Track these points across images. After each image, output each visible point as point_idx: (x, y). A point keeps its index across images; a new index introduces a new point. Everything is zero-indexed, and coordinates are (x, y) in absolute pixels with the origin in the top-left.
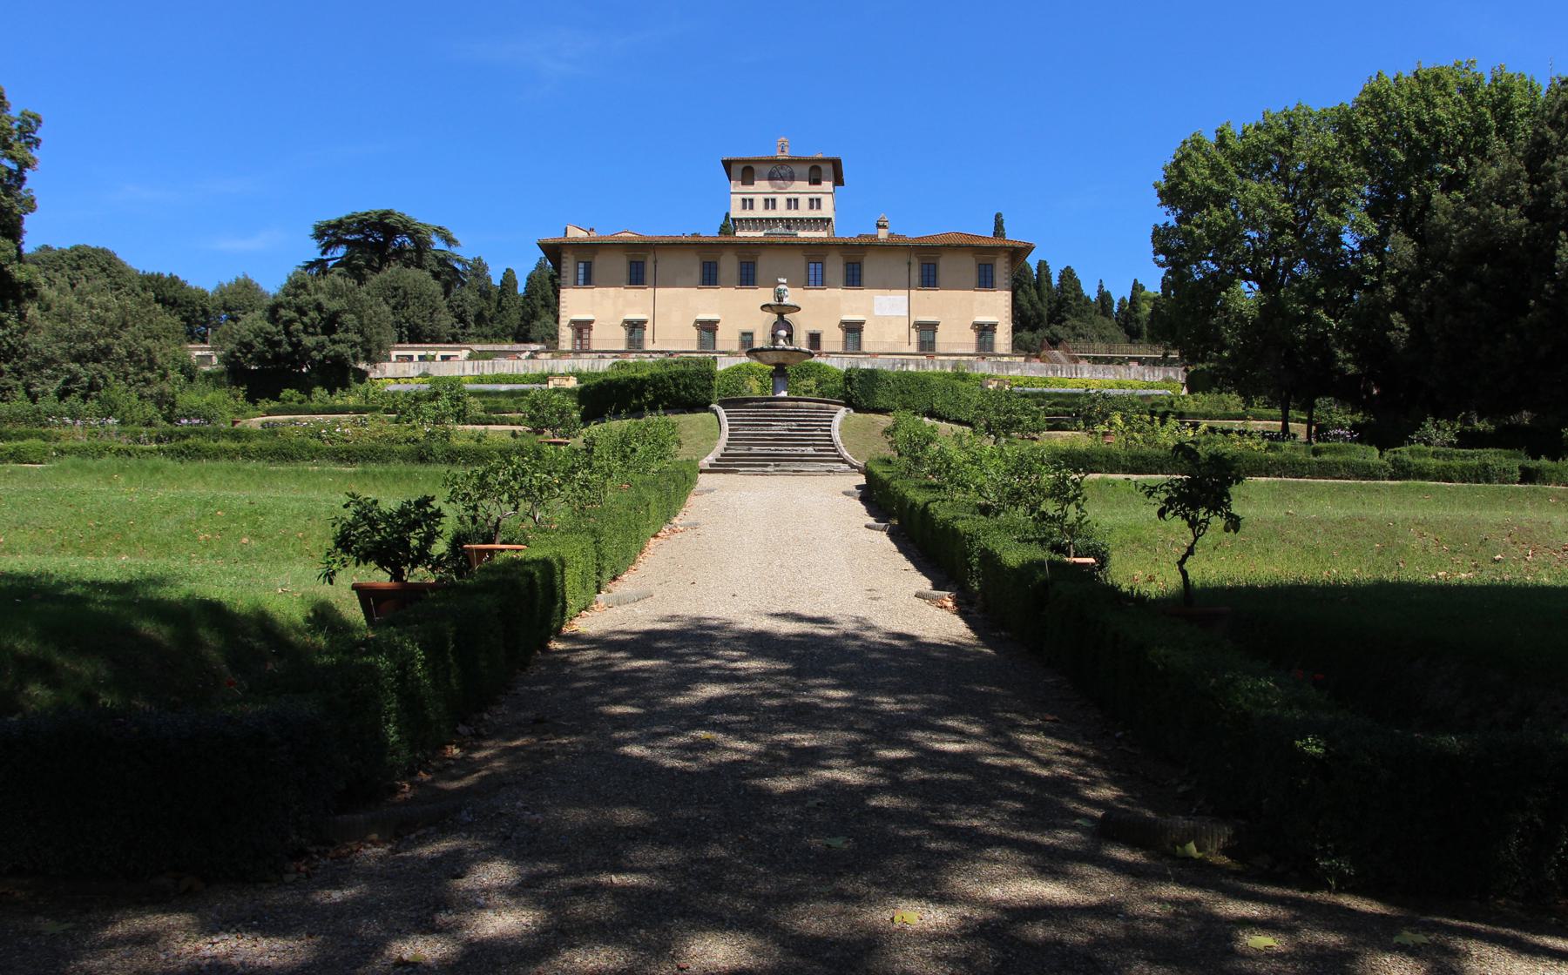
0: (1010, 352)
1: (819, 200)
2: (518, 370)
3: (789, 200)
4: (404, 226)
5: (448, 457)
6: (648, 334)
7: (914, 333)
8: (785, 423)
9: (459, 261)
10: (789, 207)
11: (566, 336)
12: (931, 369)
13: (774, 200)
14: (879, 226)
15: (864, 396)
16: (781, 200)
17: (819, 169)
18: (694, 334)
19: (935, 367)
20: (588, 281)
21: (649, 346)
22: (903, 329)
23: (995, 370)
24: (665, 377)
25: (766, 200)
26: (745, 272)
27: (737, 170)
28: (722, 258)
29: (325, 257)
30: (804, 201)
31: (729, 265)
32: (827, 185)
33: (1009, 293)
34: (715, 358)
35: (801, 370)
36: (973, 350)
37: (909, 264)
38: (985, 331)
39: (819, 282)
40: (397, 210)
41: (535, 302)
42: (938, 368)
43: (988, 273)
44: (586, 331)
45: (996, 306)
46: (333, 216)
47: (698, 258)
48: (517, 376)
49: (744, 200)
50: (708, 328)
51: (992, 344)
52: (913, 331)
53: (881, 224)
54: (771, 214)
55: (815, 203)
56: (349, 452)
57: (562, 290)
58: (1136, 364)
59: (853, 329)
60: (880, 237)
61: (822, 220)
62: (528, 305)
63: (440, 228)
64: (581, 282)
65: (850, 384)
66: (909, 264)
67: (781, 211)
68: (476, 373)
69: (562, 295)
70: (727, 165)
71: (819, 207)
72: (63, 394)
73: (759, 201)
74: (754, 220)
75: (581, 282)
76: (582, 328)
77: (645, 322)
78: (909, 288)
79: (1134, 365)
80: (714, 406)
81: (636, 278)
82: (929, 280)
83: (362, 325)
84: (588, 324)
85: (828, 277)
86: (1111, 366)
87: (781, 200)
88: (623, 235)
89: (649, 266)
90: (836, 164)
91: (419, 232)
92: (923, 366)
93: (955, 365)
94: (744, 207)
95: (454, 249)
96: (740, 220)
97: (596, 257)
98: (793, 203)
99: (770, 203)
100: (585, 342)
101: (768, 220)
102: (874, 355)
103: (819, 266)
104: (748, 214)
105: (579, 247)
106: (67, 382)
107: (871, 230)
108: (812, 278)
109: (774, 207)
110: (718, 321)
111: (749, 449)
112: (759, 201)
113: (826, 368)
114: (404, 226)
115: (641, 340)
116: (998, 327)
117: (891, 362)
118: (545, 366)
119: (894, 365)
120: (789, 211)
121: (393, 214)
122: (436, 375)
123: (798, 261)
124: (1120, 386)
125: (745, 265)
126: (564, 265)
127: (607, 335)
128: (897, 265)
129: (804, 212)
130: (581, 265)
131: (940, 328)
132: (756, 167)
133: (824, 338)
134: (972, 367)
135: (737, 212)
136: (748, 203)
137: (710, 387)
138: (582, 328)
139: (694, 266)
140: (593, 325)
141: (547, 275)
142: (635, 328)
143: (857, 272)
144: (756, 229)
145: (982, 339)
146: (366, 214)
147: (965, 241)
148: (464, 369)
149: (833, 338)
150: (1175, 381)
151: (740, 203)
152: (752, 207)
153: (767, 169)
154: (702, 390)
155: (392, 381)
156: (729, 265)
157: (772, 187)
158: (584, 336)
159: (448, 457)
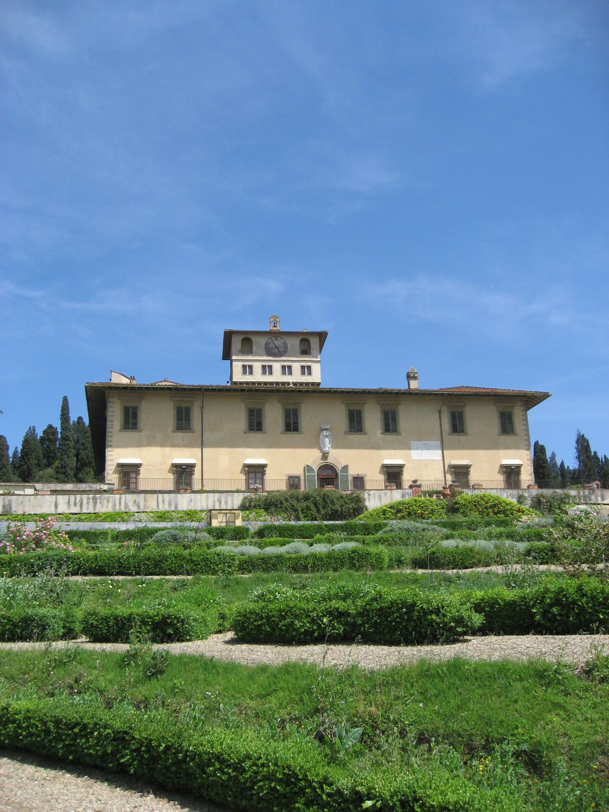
2: (126, 506)
11: (112, 476)
13: (270, 367)
16: (277, 367)
17: (308, 341)
25: (264, 367)
30: (296, 367)
37: (440, 412)
38: (511, 474)
44: (133, 475)
61: (313, 384)
66: (440, 412)
71: (310, 373)
73: (257, 367)
76: (129, 472)
77: (192, 466)
81: (183, 421)
87: (277, 367)
98: (287, 370)
109: (271, 373)
110: (264, 466)
112: (257, 367)
116: (523, 469)
131: (472, 470)
132: (254, 339)
138: (129, 472)
140: (141, 469)
148: (56, 506)
149: (375, 479)
151: (240, 369)
152: (251, 373)
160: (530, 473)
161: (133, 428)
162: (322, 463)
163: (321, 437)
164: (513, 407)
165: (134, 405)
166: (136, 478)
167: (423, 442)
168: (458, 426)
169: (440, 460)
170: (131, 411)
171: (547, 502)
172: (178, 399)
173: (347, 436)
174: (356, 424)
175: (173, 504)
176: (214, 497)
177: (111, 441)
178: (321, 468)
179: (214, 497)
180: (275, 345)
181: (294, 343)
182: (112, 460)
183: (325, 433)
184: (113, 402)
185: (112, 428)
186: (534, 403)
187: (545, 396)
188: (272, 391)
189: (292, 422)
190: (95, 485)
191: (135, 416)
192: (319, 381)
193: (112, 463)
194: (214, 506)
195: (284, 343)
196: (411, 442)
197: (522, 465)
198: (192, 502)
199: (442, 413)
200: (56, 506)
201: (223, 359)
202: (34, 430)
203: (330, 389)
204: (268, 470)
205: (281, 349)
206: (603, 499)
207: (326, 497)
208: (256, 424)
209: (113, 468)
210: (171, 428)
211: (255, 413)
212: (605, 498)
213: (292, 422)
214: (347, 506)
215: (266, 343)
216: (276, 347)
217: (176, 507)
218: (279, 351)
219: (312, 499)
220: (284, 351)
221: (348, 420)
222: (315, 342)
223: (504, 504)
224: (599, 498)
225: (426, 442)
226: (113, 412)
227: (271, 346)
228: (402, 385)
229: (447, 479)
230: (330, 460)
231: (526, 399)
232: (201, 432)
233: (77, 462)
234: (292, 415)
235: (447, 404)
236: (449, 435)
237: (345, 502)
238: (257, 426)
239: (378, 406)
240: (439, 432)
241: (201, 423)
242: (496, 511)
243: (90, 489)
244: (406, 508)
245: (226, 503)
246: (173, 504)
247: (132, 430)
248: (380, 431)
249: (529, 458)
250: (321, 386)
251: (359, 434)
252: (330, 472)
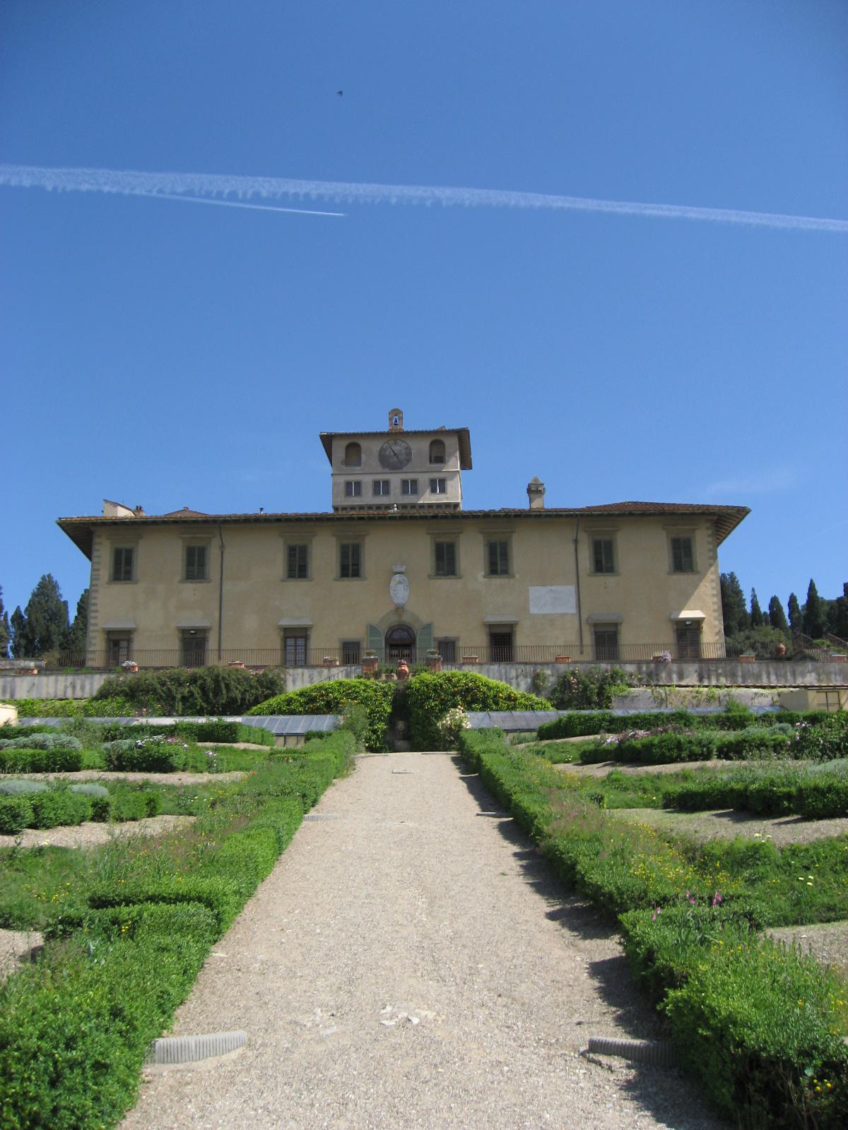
3: (405, 483)
7: (588, 639)
11: (96, 646)
22: (572, 637)
23: (773, 678)
27: (339, 448)
30: (424, 479)
37: (576, 541)
44: (123, 644)
61: (448, 505)
66: (576, 541)
70: (328, 441)
71: (443, 490)
76: (118, 641)
90: (462, 436)
97: (141, 542)
99: (381, 487)
116: (705, 626)
120: (406, 496)
132: (364, 444)
138: (118, 641)
160: (717, 630)
161: (125, 579)
162: (394, 620)
163: (393, 584)
164: (693, 530)
165: (128, 546)
166: (128, 648)
167: (549, 588)
168: (604, 561)
169: (573, 614)
170: (124, 555)
171: (578, 684)
172: (189, 536)
173: (433, 581)
174: (445, 563)
175: (9, 690)
176: (66, 680)
177: (95, 598)
178: (392, 630)
179: (66, 680)
180: (394, 452)
181: (421, 447)
182: (95, 625)
183: (397, 577)
184: (100, 544)
185: (98, 579)
186: (732, 524)
187: (741, 513)
188: (371, 519)
189: (350, 564)
190: (18, 662)
191: (129, 561)
193: (96, 628)
194: (65, 692)
195: (406, 448)
196: (530, 588)
197: (704, 618)
198: (35, 688)
199: (579, 545)
201: (471, 468)
203: (470, 512)
205: (402, 457)
206: (681, 677)
207: (220, 678)
208: (298, 567)
210: (179, 578)
211: (297, 551)
212: (685, 676)
213: (350, 564)
214: (253, 691)
215: (380, 450)
216: (395, 454)
217: (12, 695)
218: (399, 461)
219: (200, 682)
220: (407, 460)
221: (434, 558)
222: (451, 444)
223: (484, 689)
224: (675, 676)
225: (553, 588)
226: (100, 557)
227: (387, 453)
228: (521, 502)
229: (584, 643)
230: (406, 619)
231: (715, 518)
232: (219, 582)
234: (350, 554)
235: (587, 529)
236: (589, 575)
237: (251, 687)
238: (300, 571)
239: (481, 537)
240: (575, 571)
241: (220, 569)
242: (469, 698)
243: (12, 667)
244: (322, 695)
245: (83, 688)
246: (9, 690)
247: (198, 581)
248: (483, 573)
249: (716, 607)
250: (462, 508)
251: (450, 578)
252: (405, 635)
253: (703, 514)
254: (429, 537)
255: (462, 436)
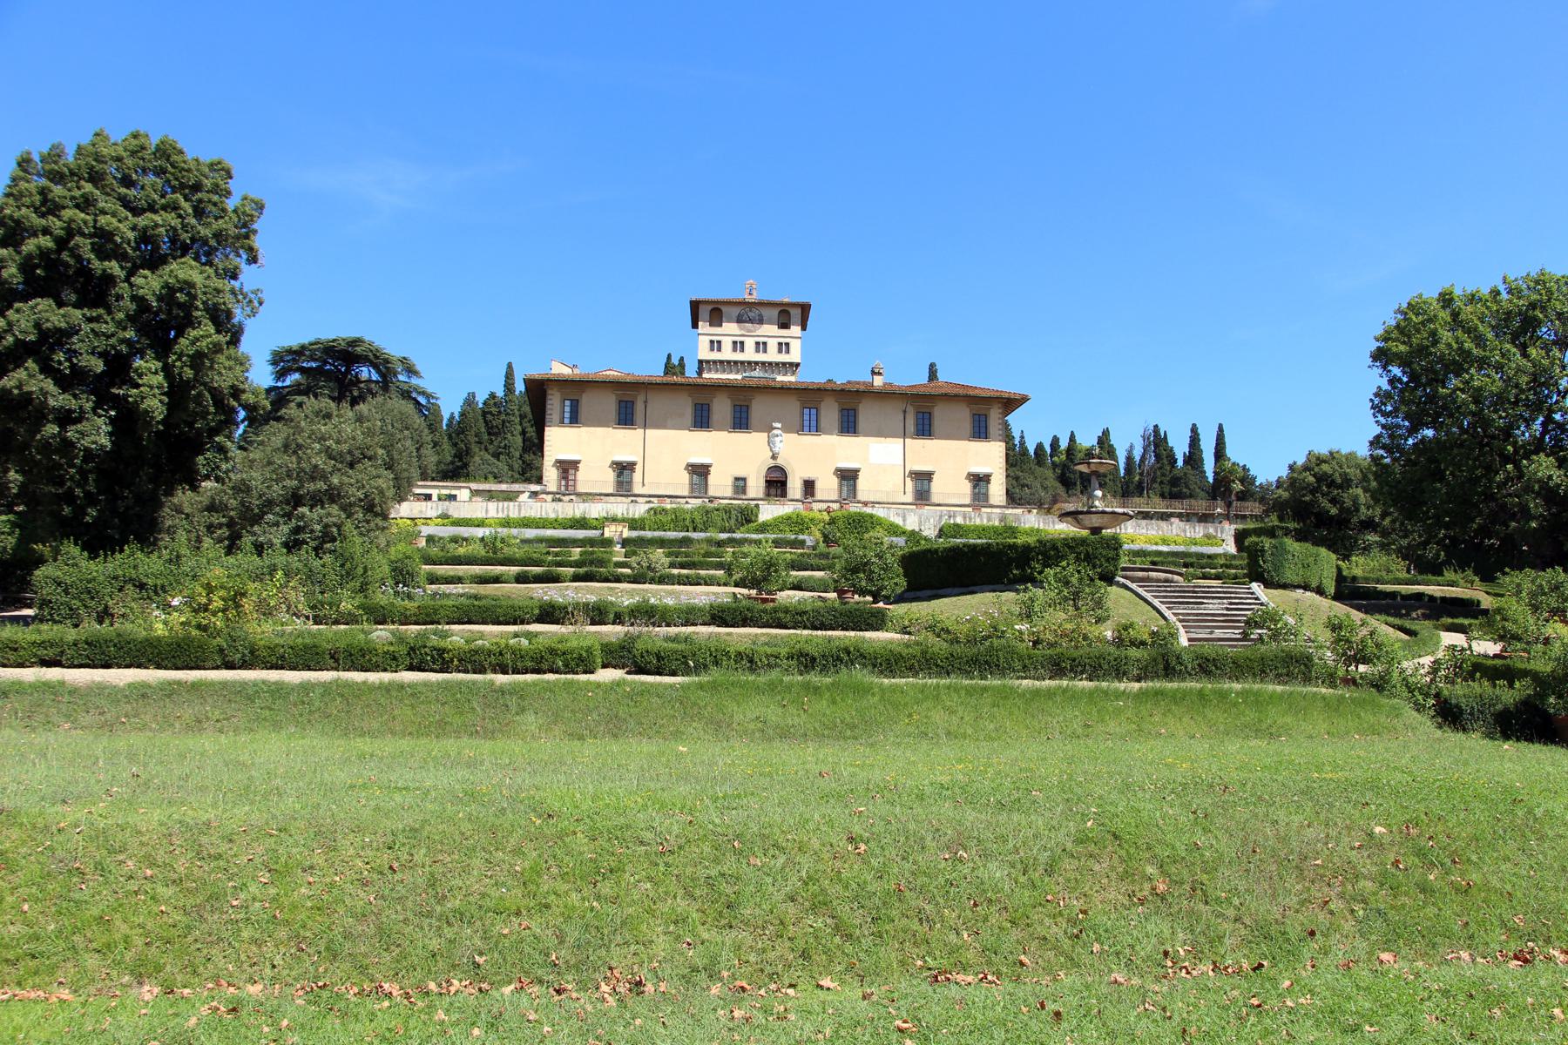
0: (1004, 503)
1: (787, 345)
3: (757, 344)
4: (374, 355)
5: (1199, 665)
6: (637, 476)
7: (909, 483)
8: (1215, 601)
9: (423, 393)
10: (757, 351)
11: (551, 475)
12: (978, 522)
14: (873, 373)
15: (1275, 570)
16: (750, 343)
17: (788, 313)
18: (685, 477)
19: (982, 520)
20: (575, 420)
21: (637, 489)
23: (1042, 524)
24: (1059, 545)
25: (735, 343)
26: (738, 415)
28: (715, 400)
29: (280, 384)
30: (772, 345)
31: (722, 408)
32: (795, 330)
33: (1003, 445)
34: (757, 506)
35: (854, 521)
36: (967, 501)
37: (905, 412)
38: (979, 481)
39: (813, 428)
40: (366, 338)
41: (469, 437)
42: (985, 521)
43: (983, 424)
45: (989, 457)
46: (294, 341)
47: (690, 400)
48: (546, 520)
49: (712, 342)
50: (700, 472)
51: (986, 495)
52: (908, 480)
53: (876, 370)
54: (739, 357)
55: (784, 347)
56: (1074, 660)
57: (546, 428)
58: (1177, 520)
59: (848, 477)
60: (875, 384)
61: (791, 364)
62: (462, 441)
63: (404, 358)
64: (567, 421)
65: (1263, 556)
66: (905, 412)
67: (750, 354)
68: (500, 515)
69: (546, 433)
70: (695, 306)
71: (788, 352)
72: (292, 546)
73: (727, 343)
74: (721, 362)
75: (567, 421)
76: (567, 468)
78: (904, 436)
79: (1175, 520)
80: (1118, 579)
81: (626, 418)
82: (925, 429)
83: (392, 459)
84: (575, 464)
85: (823, 424)
86: (1153, 521)
87: (750, 343)
88: (608, 373)
89: (639, 406)
90: (805, 309)
91: (388, 362)
92: (970, 519)
93: (1003, 518)
94: (712, 349)
95: (414, 381)
96: (708, 362)
97: (584, 395)
98: (761, 347)
99: (738, 346)
100: (571, 483)
101: (736, 362)
102: (865, 504)
103: (814, 411)
104: (716, 356)
105: (564, 383)
106: (297, 530)
107: (866, 377)
108: (806, 423)
111: (1211, 633)
112: (727, 343)
113: (879, 518)
114: (374, 355)
115: (630, 483)
116: (992, 478)
117: (938, 513)
118: (576, 511)
119: (941, 516)
121: (363, 342)
122: (456, 516)
123: (792, 406)
124: (1165, 542)
125: (738, 408)
126: (549, 402)
127: (595, 476)
128: (892, 414)
129: (772, 355)
130: (567, 403)
132: (724, 309)
133: (818, 486)
134: (1019, 520)
135: (705, 353)
136: (716, 345)
137: (1116, 558)
138: (567, 468)
139: (686, 406)
141: (480, 411)
142: (623, 470)
143: (852, 419)
144: (724, 371)
145: (977, 490)
146: (334, 341)
147: (961, 392)
148: (487, 511)
150: (1215, 537)
151: (708, 345)
152: (719, 349)
153: (735, 311)
154: (1108, 560)
155: (409, 522)
156: (722, 408)
157: (741, 329)
158: (571, 477)
159: (1199, 665)
162: (771, 463)
187: (1023, 400)
192: (797, 360)
200: (487, 511)
202: (474, 397)
204: (711, 469)
209: (552, 463)
222: (796, 313)
230: (780, 462)
233: (524, 441)
253: (997, 398)
254: (798, 403)
255: (805, 309)
